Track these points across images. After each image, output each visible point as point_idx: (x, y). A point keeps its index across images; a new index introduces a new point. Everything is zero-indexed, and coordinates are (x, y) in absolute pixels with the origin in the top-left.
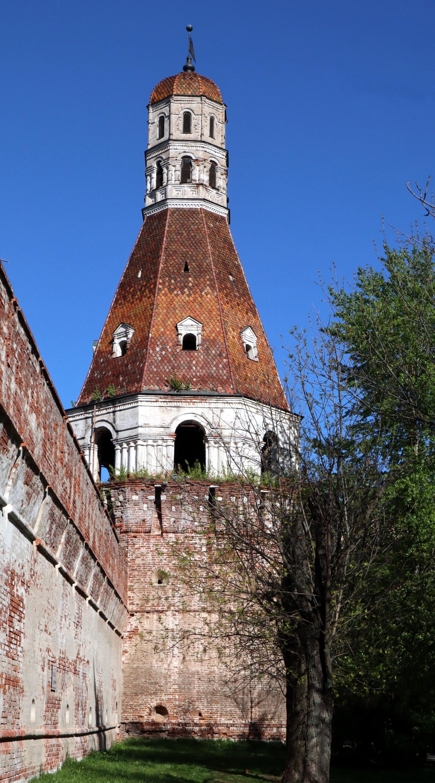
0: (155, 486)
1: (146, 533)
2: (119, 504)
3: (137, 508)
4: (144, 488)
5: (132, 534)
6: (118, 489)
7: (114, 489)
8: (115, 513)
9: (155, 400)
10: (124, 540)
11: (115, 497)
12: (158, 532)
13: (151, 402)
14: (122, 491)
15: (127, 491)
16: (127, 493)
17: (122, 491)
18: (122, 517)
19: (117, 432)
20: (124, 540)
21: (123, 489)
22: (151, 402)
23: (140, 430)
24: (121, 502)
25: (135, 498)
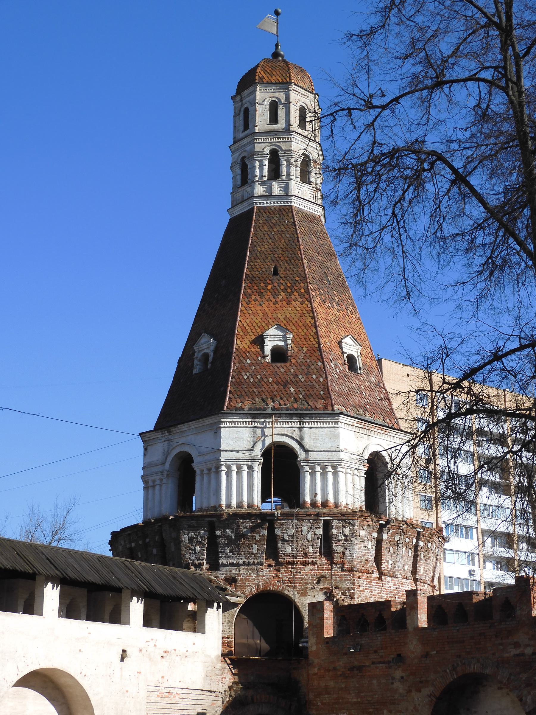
0: (380, 522)
1: (369, 573)
2: (343, 538)
3: (363, 545)
4: (371, 523)
5: (358, 574)
6: (345, 520)
7: (339, 520)
8: (335, 548)
9: (351, 424)
10: (348, 580)
11: (338, 528)
12: (376, 574)
13: (348, 424)
14: (349, 523)
15: (356, 524)
16: (356, 527)
17: (349, 523)
18: (344, 553)
19: (307, 451)
20: (348, 580)
21: (351, 521)
22: (348, 424)
23: (342, 455)
24: (345, 536)
25: (363, 533)
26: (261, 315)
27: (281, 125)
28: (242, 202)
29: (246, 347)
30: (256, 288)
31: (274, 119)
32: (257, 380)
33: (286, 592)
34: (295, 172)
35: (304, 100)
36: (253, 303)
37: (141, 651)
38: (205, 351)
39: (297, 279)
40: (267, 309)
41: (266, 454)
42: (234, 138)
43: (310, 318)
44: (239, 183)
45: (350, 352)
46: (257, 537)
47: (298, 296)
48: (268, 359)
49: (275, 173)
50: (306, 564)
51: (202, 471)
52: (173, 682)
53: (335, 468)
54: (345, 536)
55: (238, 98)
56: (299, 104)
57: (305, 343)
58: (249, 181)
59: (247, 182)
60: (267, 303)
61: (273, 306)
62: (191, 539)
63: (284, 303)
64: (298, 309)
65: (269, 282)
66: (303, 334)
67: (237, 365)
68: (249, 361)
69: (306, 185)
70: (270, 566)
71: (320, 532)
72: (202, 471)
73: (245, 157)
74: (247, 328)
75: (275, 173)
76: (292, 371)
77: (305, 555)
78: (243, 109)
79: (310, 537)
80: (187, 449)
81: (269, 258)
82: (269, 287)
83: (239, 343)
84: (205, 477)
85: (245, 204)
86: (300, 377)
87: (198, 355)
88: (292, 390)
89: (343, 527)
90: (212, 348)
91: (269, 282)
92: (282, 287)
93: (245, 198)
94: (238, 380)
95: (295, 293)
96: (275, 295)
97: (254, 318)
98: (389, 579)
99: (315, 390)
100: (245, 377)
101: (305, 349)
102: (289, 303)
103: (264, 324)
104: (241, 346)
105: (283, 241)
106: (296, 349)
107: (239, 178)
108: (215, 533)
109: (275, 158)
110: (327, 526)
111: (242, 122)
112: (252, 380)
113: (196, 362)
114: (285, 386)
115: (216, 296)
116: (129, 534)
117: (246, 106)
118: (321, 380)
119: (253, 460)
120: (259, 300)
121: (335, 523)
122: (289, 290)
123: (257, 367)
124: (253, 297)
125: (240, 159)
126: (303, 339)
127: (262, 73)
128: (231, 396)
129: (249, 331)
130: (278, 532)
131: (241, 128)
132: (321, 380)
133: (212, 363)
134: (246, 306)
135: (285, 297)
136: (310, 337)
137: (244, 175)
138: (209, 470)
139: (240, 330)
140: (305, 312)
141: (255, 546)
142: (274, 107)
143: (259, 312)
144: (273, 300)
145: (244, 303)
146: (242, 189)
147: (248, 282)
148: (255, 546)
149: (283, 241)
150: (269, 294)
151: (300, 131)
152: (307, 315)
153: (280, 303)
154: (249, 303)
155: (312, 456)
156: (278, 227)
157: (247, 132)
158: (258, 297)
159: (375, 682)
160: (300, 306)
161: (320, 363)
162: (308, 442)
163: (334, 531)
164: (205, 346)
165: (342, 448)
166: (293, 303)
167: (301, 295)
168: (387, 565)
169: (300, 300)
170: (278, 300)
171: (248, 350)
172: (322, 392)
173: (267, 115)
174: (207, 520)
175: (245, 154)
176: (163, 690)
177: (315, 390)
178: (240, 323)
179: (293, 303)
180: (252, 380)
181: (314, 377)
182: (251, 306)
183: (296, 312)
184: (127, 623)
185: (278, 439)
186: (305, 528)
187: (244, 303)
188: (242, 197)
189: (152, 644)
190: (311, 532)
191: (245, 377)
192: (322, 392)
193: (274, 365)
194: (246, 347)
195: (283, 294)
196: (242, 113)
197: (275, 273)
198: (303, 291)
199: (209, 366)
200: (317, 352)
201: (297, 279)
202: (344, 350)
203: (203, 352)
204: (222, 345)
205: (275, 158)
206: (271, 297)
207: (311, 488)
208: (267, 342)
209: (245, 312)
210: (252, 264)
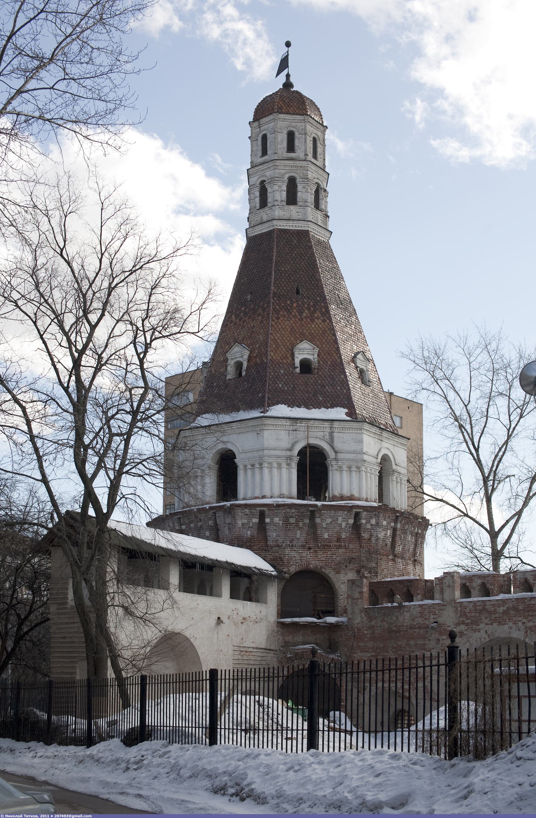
8: (363, 535)
19: (336, 452)
23: (365, 457)
25: (385, 523)
26: (289, 330)
27: (299, 153)
28: (262, 223)
29: (278, 358)
30: (283, 305)
31: (291, 148)
32: (290, 389)
33: (323, 570)
34: (311, 198)
35: (315, 131)
36: (282, 318)
37: (229, 618)
38: (238, 359)
39: (318, 299)
40: (294, 325)
41: (302, 453)
42: (252, 162)
43: (331, 335)
44: (258, 205)
45: (361, 367)
46: (301, 524)
47: (320, 315)
48: (298, 370)
49: (292, 198)
50: (340, 547)
51: (245, 466)
52: (248, 643)
53: (358, 468)
54: (371, 525)
55: (256, 124)
56: (313, 135)
57: (329, 357)
58: (269, 205)
59: (267, 205)
60: (293, 319)
61: (299, 322)
62: (243, 524)
63: (309, 320)
64: (321, 326)
65: (294, 300)
66: (326, 349)
67: (273, 374)
68: (282, 372)
69: (319, 212)
70: (310, 549)
71: (351, 521)
72: (245, 466)
73: (265, 181)
74: (278, 341)
75: (292, 198)
76: (320, 382)
77: (339, 539)
78: (261, 135)
79: (344, 525)
80: (230, 447)
81: (292, 278)
82: (295, 305)
83: (272, 354)
84: (249, 472)
85: (266, 225)
86: (327, 388)
87: (231, 363)
88: (321, 399)
89: (371, 518)
90: (246, 357)
91: (294, 300)
92: (306, 306)
93: (265, 219)
94: (274, 388)
95: (318, 312)
96: (301, 313)
97: (284, 333)
98: (400, 560)
99: (340, 400)
100: (280, 385)
101: (329, 363)
102: (312, 320)
103: (292, 339)
104: (274, 358)
105: (303, 263)
106: (321, 363)
107: (258, 200)
108: (264, 520)
109: (292, 184)
110: (357, 516)
111: (260, 148)
112: (286, 389)
113: (229, 368)
114: (315, 395)
115: (243, 309)
116: (179, 518)
117: (264, 132)
118: (345, 391)
119: (290, 458)
120: (287, 316)
121: (364, 514)
122: (312, 309)
123: (290, 377)
124: (281, 313)
125: (258, 182)
126: (327, 354)
127: (281, 103)
128: (270, 401)
129: (280, 344)
130: (318, 520)
131: (260, 153)
132: (345, 391)
133: (247, 371)
134: (276, 321)
135: (309, 315)
136: (333, 352)
137: (261, 196)
138: (253, 465)
139: (272, 343)
140: (327, 329)
141: (299, 532)
142: (291, 136)
143: (287, 327)
144: (299, 317)
145: (274, 318)
146: (261, 211)
147: (275, 299)
148: (299, 532)
149: (303, 263)
150: (295, 311)
151: (313, 160)
152: (328, 332)
153: (305, 320)
154: (278, 318)
155: (340, 456)
156: (297, 250)
157: (266, 158)
158: (286, 313)
159: (412, 642)
160: (323, 324)
161: (343, 376)
162: (338, 444)
163: (364, 521)
164: (238, 355)
165: (364, 451)
166: (316, 320)
167: (323, 314)
168: (399, 549)
169: (322, 318)
170: (302, 317)
171: (281, 361)
172: (346, 402)
173: (285, 144)
174: (258, 509)
175: (265, 179)
176: (242, 649)
177: (340, 400)
178: (272, 337)
179: (316, 320)
180: (286, 389)
181: (339, 388)
182: (280, 321)
183: (319, 329)
184: (219, 595)
185: (312, 441)
186: (340, 519)
187: (274, 318)
188: (262, 219)
189: (235, 612)
190: (345, 522)
191: (280, 385)
192: (346, 402)
193: (304, 375)
194: (278, 358)
195: (306, 311)
196: (260, 139)
197: (298, 292)
198: (323, 310)
199: (244, 373)
200: (338, 366)
201: (318, 299)
202: (359, 365)
203: (236, 360)
204: (255, 355)
205: (292, 184)
206: (297, 314)
207: (339, 483)
208: (296, 355)
209: (276, 326)
210: (277, 282)
